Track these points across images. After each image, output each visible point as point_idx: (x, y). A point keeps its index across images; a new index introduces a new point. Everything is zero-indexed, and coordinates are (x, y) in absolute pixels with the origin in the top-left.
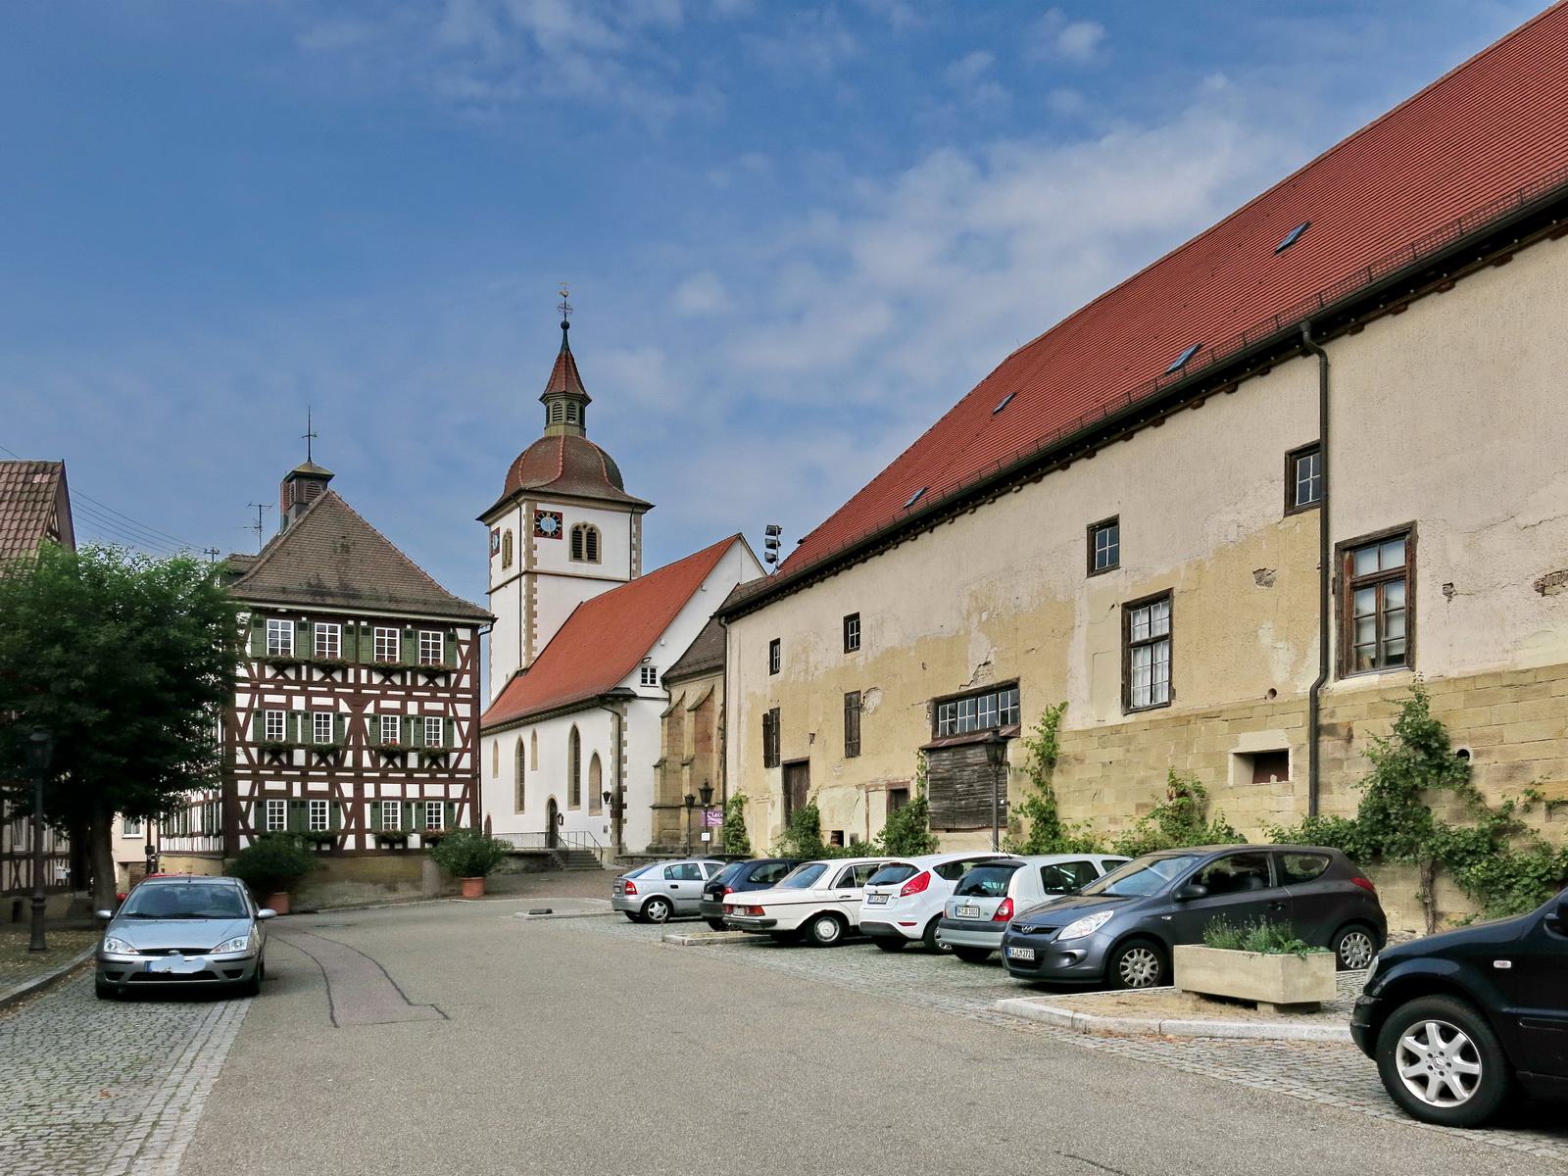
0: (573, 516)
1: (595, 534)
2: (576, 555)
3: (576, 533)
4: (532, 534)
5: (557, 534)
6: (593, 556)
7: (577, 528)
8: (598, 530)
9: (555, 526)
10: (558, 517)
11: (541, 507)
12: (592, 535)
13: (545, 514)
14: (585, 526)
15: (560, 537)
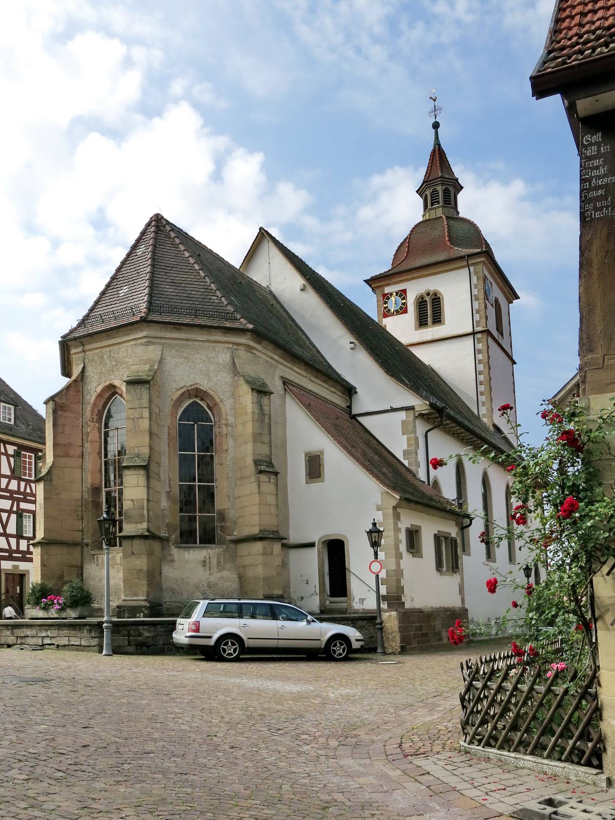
0: (415, 289)
1: (439, 298)
2: (422, 322)
3: (421, 303)
4: (382, 316)
5: (403, 310)
6: (438, 319)
7: (422, 297)
8: (441, 294)
9: (400, 301)
10: (403, 294)
11: (387, 290)
12: (437, 300)
13: (391, 294)
14: (428, 294)
15: (405, 311)
